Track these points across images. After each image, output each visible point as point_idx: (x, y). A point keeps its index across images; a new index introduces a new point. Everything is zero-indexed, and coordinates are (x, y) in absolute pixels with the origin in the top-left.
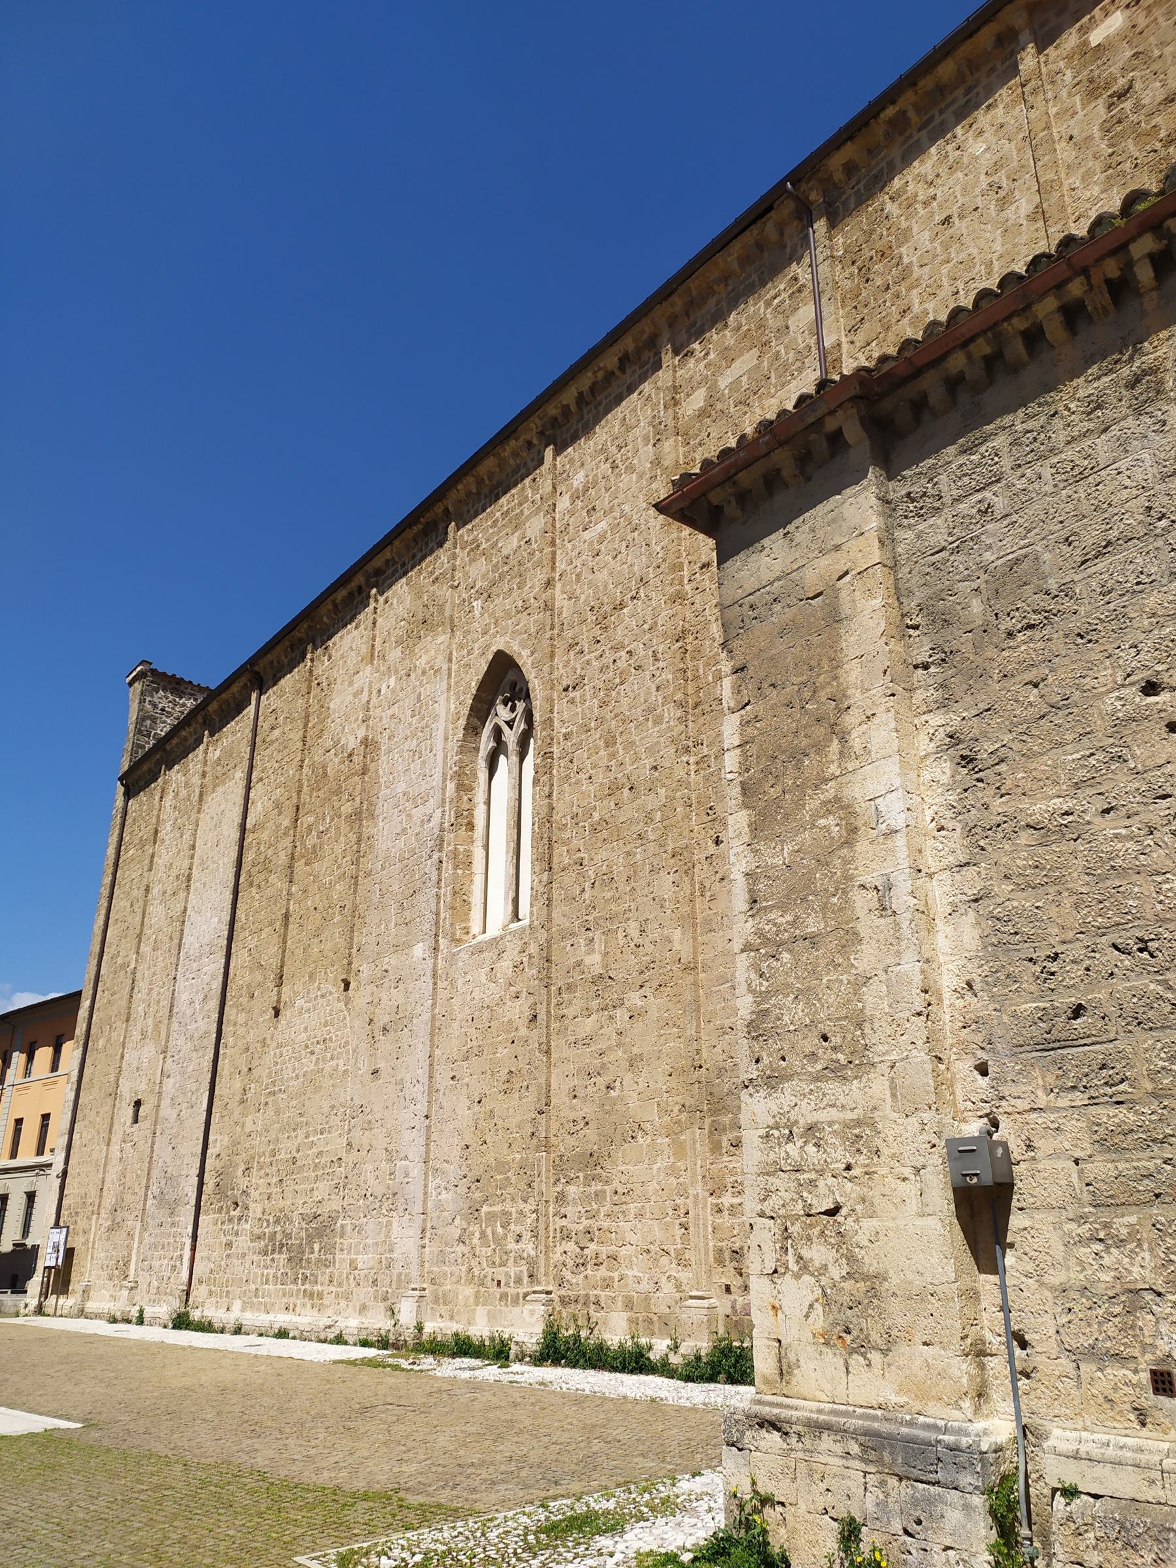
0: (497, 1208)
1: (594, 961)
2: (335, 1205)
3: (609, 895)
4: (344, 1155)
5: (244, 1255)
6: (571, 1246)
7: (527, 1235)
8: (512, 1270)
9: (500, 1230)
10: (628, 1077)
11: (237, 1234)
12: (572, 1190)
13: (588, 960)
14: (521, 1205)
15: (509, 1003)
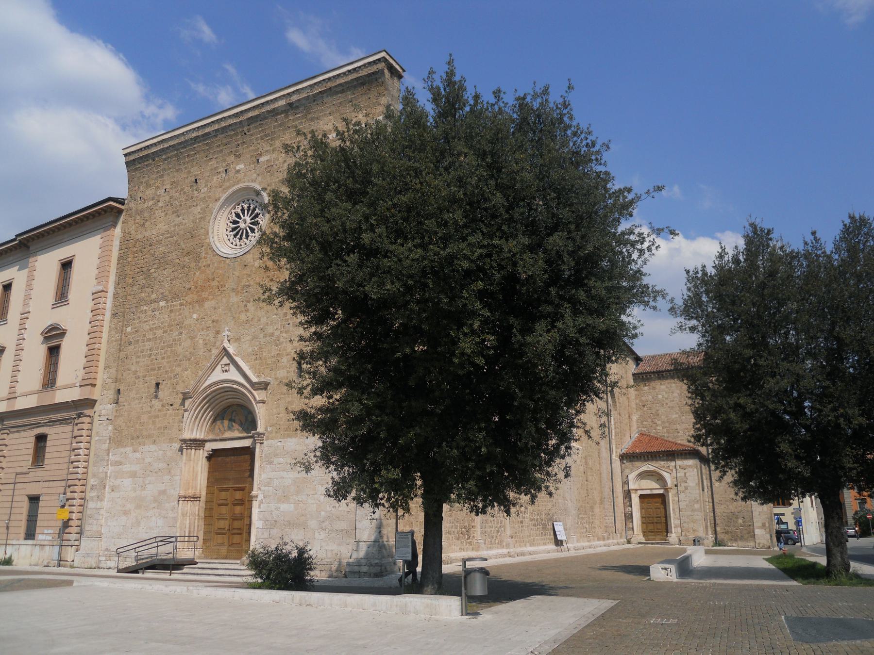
5: (528, 526)
11: (524, 518)
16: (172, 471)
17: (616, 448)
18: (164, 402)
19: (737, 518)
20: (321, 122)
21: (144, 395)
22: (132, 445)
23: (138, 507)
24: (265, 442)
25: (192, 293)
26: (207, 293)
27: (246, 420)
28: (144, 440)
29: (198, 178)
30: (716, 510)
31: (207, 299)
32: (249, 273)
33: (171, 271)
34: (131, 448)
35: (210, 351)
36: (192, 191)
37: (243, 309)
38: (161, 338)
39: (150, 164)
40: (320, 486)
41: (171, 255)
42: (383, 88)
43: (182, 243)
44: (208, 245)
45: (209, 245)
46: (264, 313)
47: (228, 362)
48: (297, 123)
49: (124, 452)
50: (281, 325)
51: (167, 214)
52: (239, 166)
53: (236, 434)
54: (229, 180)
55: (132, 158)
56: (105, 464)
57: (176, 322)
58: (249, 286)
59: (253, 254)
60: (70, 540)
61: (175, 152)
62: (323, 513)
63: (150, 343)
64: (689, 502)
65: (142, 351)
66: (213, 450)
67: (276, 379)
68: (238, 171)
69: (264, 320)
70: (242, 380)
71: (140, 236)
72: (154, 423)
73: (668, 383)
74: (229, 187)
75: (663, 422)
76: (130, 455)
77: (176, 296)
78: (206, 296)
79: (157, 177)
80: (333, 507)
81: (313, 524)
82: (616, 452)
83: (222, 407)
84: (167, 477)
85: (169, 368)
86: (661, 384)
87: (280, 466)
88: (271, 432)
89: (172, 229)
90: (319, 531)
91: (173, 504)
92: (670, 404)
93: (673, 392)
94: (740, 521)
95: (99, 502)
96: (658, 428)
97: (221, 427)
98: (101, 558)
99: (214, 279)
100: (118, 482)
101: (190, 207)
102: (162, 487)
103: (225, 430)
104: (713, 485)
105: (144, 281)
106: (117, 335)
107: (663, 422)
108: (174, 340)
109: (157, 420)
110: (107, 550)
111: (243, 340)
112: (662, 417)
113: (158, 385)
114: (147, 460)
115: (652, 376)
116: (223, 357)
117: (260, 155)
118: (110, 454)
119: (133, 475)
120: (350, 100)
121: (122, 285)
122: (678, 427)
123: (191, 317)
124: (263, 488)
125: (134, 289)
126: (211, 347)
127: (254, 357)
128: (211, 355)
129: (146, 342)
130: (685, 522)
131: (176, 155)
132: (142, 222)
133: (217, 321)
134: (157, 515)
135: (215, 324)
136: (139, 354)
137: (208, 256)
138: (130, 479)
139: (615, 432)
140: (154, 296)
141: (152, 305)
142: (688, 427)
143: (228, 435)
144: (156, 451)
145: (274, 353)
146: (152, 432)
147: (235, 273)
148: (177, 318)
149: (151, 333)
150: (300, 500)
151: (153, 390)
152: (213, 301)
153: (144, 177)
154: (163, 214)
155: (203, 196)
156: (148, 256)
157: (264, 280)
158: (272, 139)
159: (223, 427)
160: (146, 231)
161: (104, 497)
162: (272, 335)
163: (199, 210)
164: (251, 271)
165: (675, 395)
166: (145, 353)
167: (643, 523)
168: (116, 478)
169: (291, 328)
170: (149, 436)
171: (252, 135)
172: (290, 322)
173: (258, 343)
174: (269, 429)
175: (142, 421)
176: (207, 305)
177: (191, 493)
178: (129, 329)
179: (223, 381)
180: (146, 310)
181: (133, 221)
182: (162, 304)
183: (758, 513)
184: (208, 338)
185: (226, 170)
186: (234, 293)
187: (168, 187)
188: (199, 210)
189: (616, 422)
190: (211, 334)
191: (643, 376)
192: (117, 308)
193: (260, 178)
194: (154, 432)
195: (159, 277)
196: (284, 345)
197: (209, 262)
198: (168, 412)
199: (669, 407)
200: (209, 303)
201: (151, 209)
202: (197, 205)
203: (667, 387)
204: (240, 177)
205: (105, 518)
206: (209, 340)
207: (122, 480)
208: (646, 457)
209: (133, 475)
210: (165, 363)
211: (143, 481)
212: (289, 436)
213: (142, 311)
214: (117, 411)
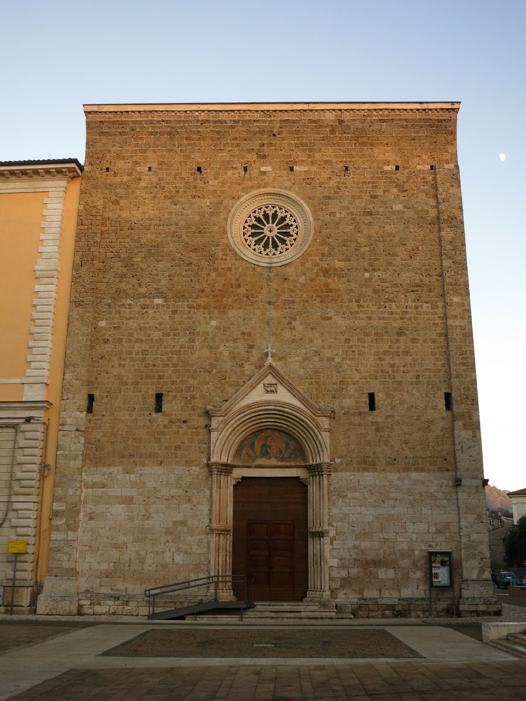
16: (194, 499)
18: (173, 417)
20: (376, 150)
21: (137, 406)
22: (122, 464)
23: (139, 540)
24: (333, 474)
25: (207, 296)
26: (230, 300)
27: (287, 447)
28: (142, 460)
29: (202, 166)
31: (231, 307)
32: (292, 288)
33: (169, 265)
34: (121, 468)
35: (241, 366)
36: (196, 179)
37: (287, 326)
38: (161, 341)
39: (125, 133)
40: (411, 524)
41: (167, 246)
42: (451, 137)
43: (184, 236)
44: (227, 246)
45: (228, 245)
46: (317, 335)
47: (275, 381)
48: (345, 142)
49: (108, 472)
50: (343, 351)
51: (155, 197)
52: (265, 167)
53: (274, 462)
54: (251, 179)
55: (98, 118)
56: (78, 485)
57: (183, 326)
58: (293, 302)
59: (295, 268)
60: (25, 580)
61: (169, 129)
62: (417, 553)
63: (144, 346)
65: (130, 353)
66: (243, 478)
67: (342, 408)
68: (264, 173)
69: (318, 342)
70: (298, 404)
71: (110, 214)
72: (158, 441)
74: (252, 188)
76: (120, 477)
77: (180, 296)
78: (230, 303)
79: (136, 151)
80: (429, 546)
81: (404, 563)
83: (253, 431)
84: (185, 507)
85: (177, 378)
87: (356, 501)
88: (341, 464)
89: (167, 216)
90: (414, 570)
91: (199, 537)
95: (70, 533)
97: (250, 452)
98: (82, 602)
99: (239, 286)
100: (100, 508)
101: (194, 197)
102: (180, 518)
103: (256, 457)
105: (124, 270)
106: (85, 328)
108: (181, 347)
109: (163, 437)
110: (87, 591)
111: (289, 360)
113: (159, 398)
114: (150, 485)
116: (267, 376)
117: (295, 163)
118: (83, 474)
119: (129, 501)
120: (413, 138)
121: (88, 268)
123: (208, 324)
124: (334, 523)
125: (108, 276)
126: (243, 362)
127: (308, 381)
128: (243, 371)
129: (135, 342)
131: (169, 133)
132: (114, 198)
133: (249, 334)
134: (173, 550)
135: (246, 336)
136: (124, 356)
137: (228, 258)
138: (123, 506)
140: (143, 290)
141: (141, 300)
143: (260, 461)
144: (164, 474)
145: (336, 378)
146: (156, 451)
147: (271, 284)
148: (186, 321)
149: (143, 333)
150: (386, 537)
151: (152, 401)
152: (240, 311)
153: (114, 146)
154: (148, 196)
155: (212, 188)
156: (128, 240)
157: (314, 299)
158: (310, 151)
159: (254, 452)
160: (121, 210)
161: (79, 526)
162: (331, 360)
163: (208, 204)
164: (295, 286)
166: (133, 356)
168: (97, 503)
169: (357, 356)
170: (151, 456)
171: (283, 139)
172: (354, 349)
173: (311, 366)
174: (337, 461)
175: (137, 436)
176: (231, 313)
177: (222, 525)
178: (102, 324)
179: (268, 403)
180: (130, 305)
181: (100, 195)
182: (158, 301)
184: (237, 351)
185: (245, 169)
186: (272, 307)
187: (154, 166)
188: (208, 204)
190: (241, 348)
192: (81, 295)
193: (296, 188)
194: (160, 452)
195: (150, 269)
196: (349, 372)
197: (230, 266)
198: (181, 430)
200: (234, 311)
201: (127, 186)
202: (203, 197)
204: (266, 180)
205: (81, 552)
206: (239, 353)
207: (108, 506)
209: (129, 501)
210: (170, 372)
211: (146, 510)
212: (364, 470)
213: (124, 305)
214: (90, 421)
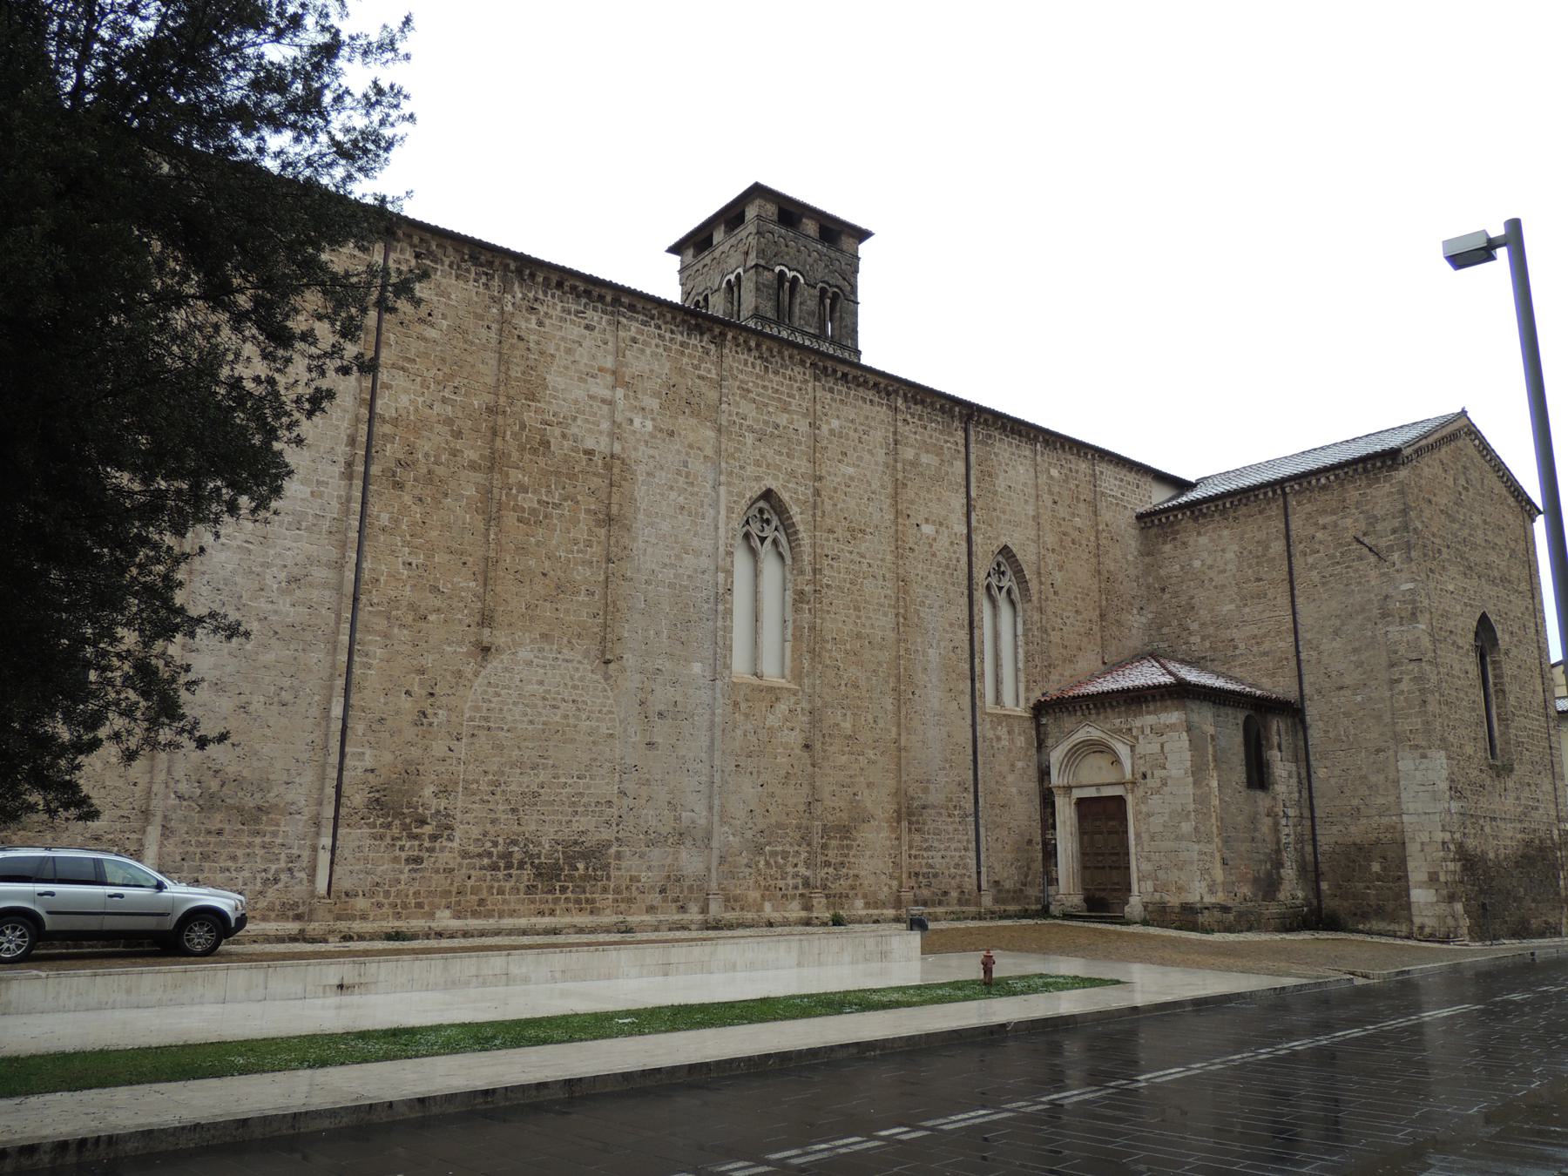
0: (779, 848)
1: (847, 726)
2: (606, 834)
3: (856, 695)
4: (615, 800)
6: (831, 870)
7: (801, 864)
8: (791, 882)
9: (781, 861)
10: (866, 792)
11: (431, 850)
12: (834, 843)
13: (843, 725)
14: (796, 848)
15: (786, 732)
17: (1028, 689)
19: (1369, 859)
30: (1318, 838)
64: (1170, 817)
73: (1214, 530)
75: (1203, 625)
82: (1027, 700)
86: (1199, 534)
92: (1219, 580)
93: (1223, 550)
94: (1376, 867)
96: (1193, 639)
104: (1313, 775)
107: (1203, 625)
112: (1201, 612)
115: (1180, 516)
122: (1235, 633)
130: (1160, 868)
139: (1026, 652)
142: (1256, 632)
165: (1230, 555)
167: (1084, 868)
183: (1419, 847)
189: (1029, 630)
191: (1160, 520)
199: (1216, 587)
203: (1212, 540)
208: (1084, 707)
